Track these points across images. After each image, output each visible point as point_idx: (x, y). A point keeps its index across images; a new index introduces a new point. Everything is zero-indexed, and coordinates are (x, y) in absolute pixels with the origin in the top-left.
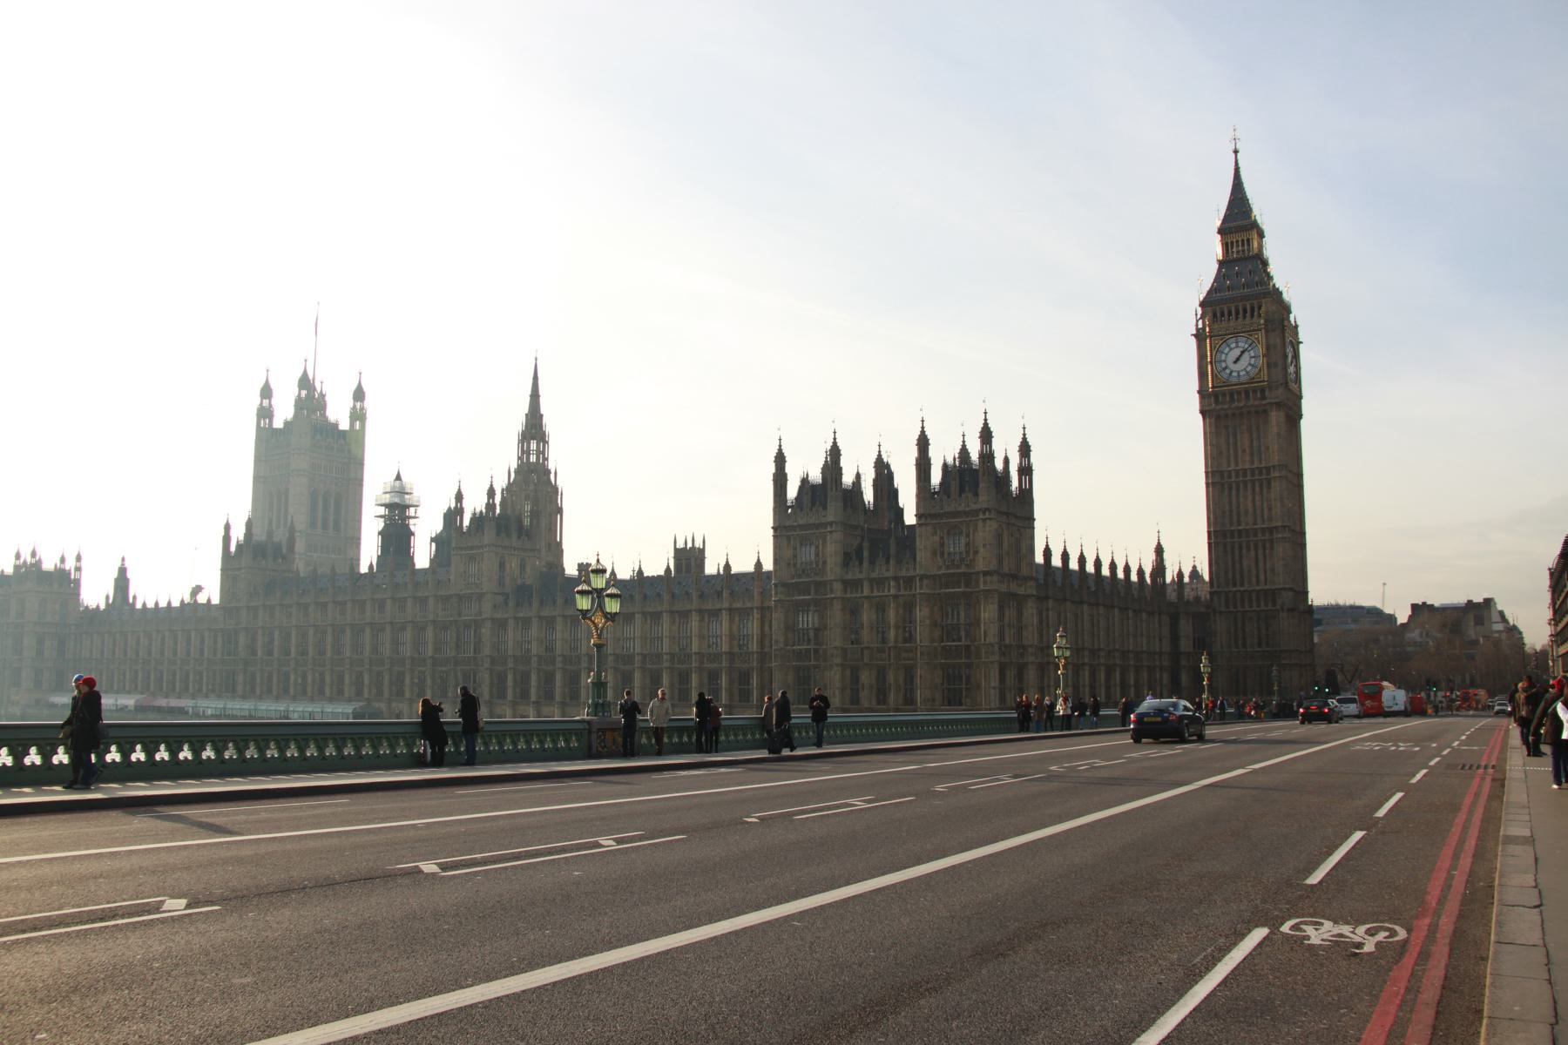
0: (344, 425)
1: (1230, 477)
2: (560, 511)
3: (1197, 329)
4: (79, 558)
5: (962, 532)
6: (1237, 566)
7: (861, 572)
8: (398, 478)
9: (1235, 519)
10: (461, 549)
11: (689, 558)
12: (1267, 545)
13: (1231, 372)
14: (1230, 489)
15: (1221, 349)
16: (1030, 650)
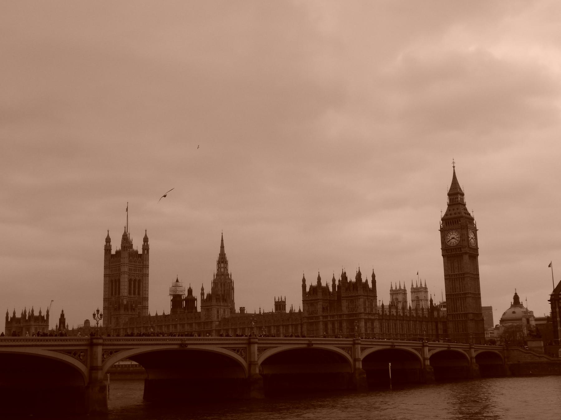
0: (140, 252)
1: (452, 276)
2: (233, 289)
3: (441, 228)
4: (48, 312)
5: (354, 302)
6: (455, 305)
7: (327, 313)
8: (177, 281)
9: (454, 290)
10: (204, 306)
11: (280, 305)
12: (464, 298)
13: (451, 242)
14: (452, 280)
15: (448, 235)
16: (377, 335)
